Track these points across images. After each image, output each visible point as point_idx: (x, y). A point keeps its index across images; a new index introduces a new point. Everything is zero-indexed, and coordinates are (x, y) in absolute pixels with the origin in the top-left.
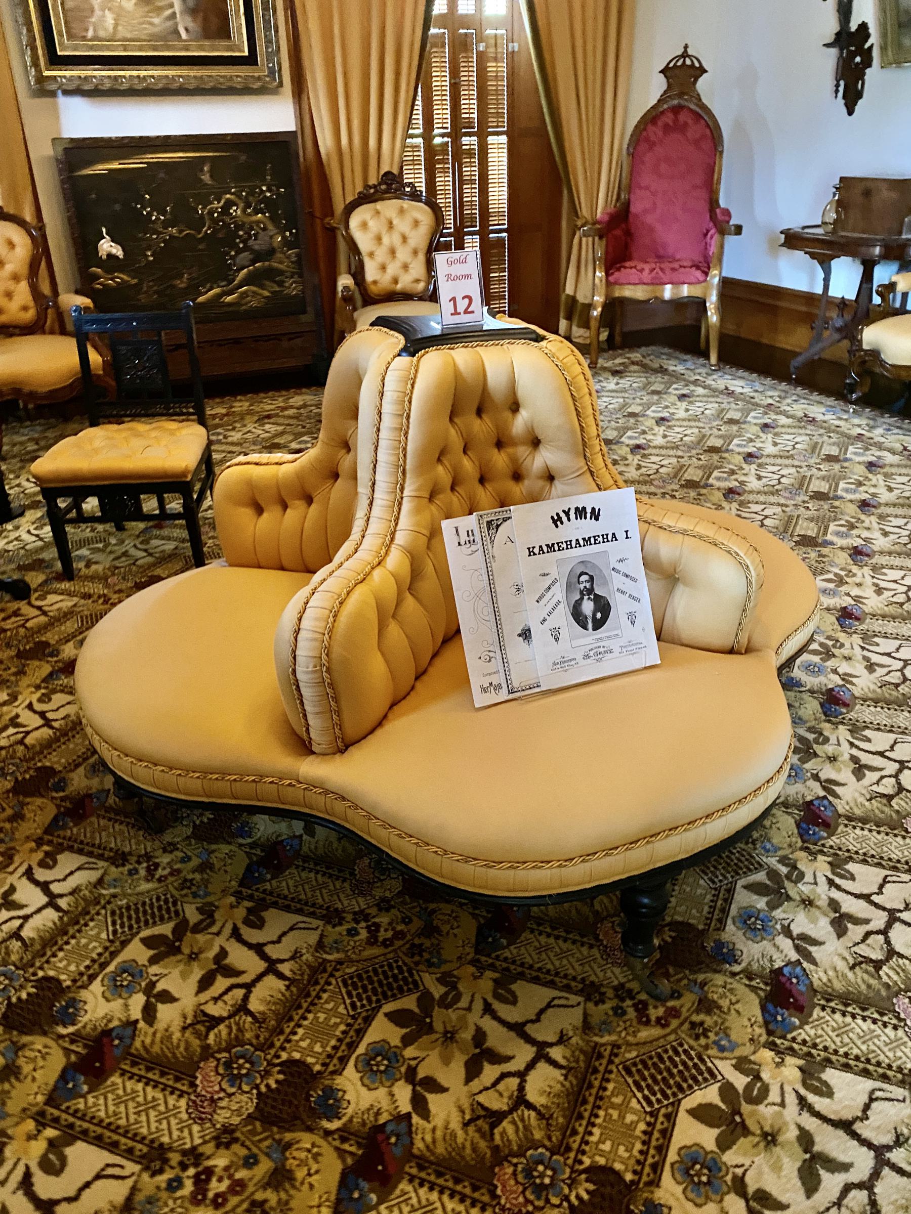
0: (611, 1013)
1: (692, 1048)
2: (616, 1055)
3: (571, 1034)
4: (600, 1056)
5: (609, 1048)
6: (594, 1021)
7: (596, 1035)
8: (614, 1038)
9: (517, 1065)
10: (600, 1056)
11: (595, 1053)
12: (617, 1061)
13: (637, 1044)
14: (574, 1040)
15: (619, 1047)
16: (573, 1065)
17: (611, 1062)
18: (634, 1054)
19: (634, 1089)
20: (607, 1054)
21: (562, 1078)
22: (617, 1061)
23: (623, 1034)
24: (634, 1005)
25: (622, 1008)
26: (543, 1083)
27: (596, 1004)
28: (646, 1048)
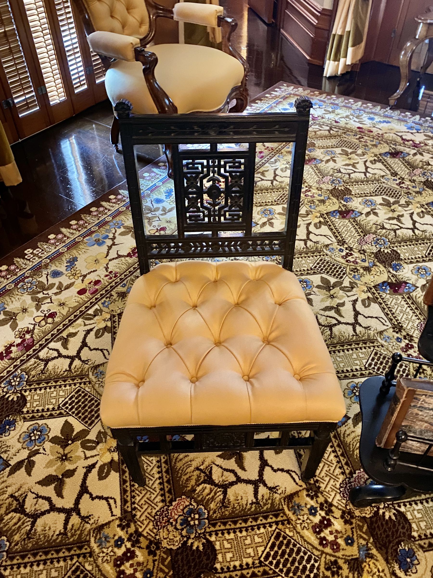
0: (308, 506)
1: (318, 569)
2: (283, 524)
5: (285, 518)
7: (288, 507)
8: (293, 518)
10: (276, 516)
14: (276, 495)
15: (289, 523)
18: (291, 534)
20: (280, 519)
22: (280, 526)
23: (298, 522)
24: (324, 518)
25: (316, 511)
27: (308, 495)
28: (300, 540)
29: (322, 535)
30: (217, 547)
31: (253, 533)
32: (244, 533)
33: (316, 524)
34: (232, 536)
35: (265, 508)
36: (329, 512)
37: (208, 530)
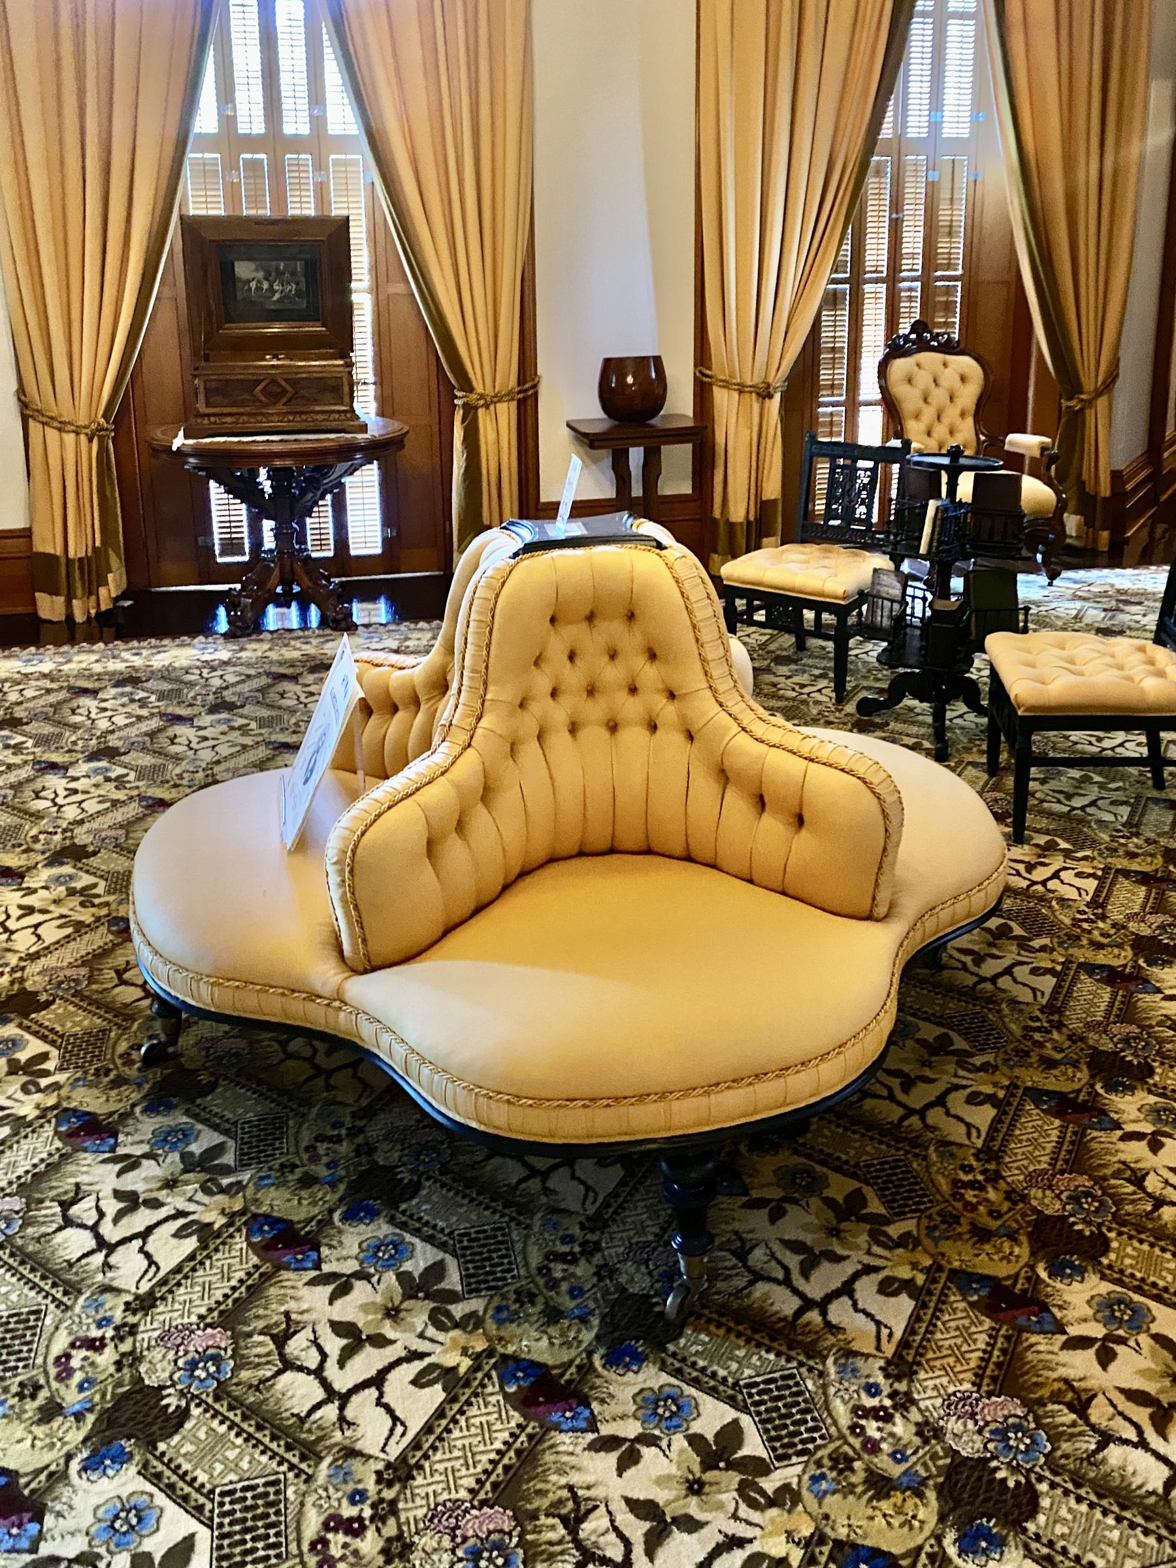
2: (297, 1476)
3: (348, 1433)
4: (303, 1458)
6: (356, 1465)
9: (331, 1370)
10: (303, 1458)
11: (311, 1453)
12: (291, 1475)
13: (302, 1504)
14: (338, 1434)
15: (306, 1481)
16: (307, 1426)
17: (292, 1467)
19: (246, 1483)
20: (303, 1466)
21: (295, 1411)
26: (298, 1393)
29: (330, 1536)
30: (188, 1425)
31: (250, 1450)
32: (239, 1441)
33: (340, 1516)
34: (223, 1429)
35: (304, 1436)
36: (379, 1518)
37: (204, 1396)
